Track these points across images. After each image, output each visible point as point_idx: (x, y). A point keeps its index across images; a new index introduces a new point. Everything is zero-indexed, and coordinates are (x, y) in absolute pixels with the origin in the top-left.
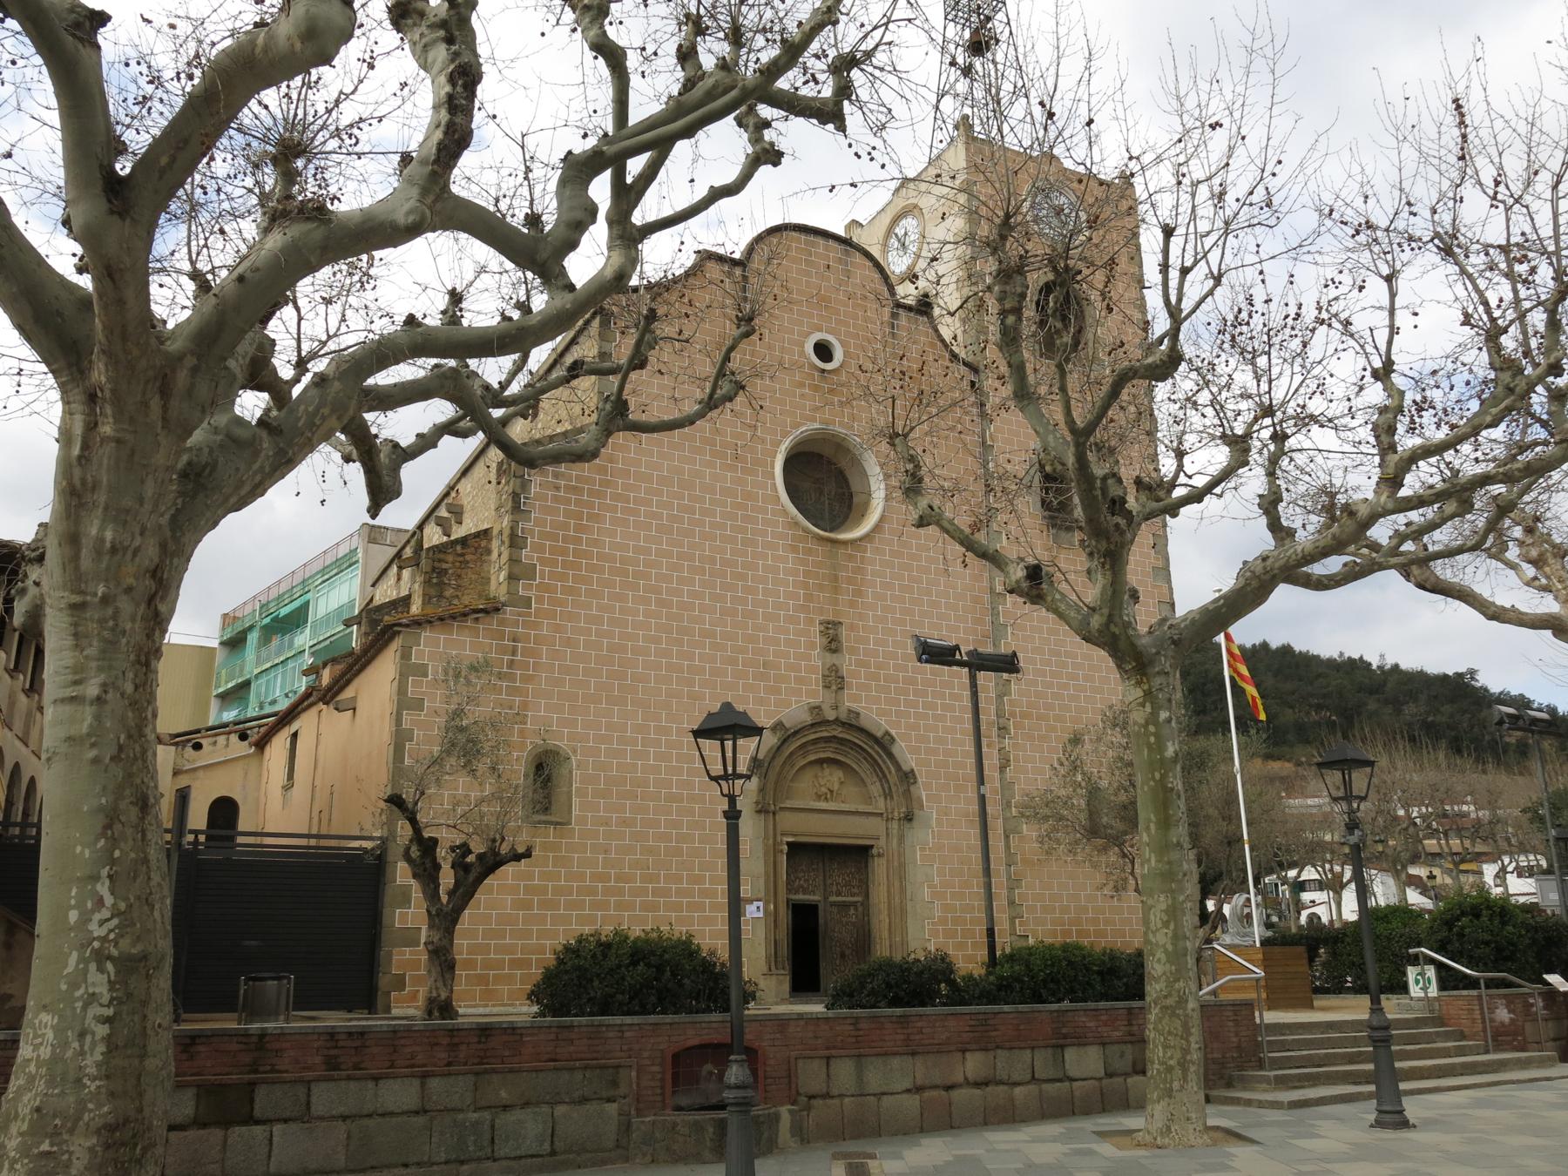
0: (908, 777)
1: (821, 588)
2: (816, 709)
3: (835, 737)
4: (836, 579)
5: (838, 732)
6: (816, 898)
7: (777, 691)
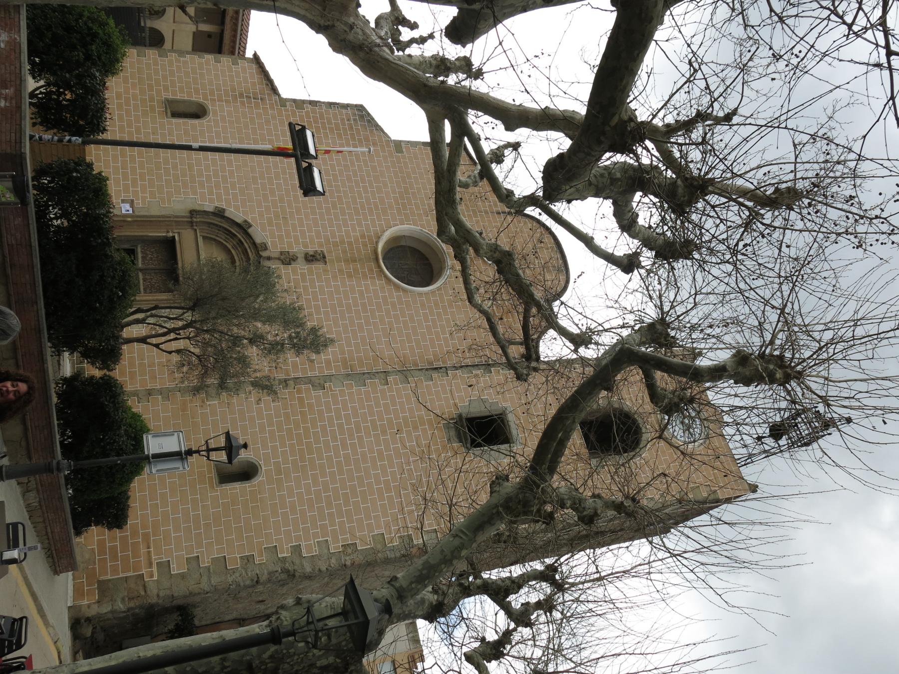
1: (344, 252)
2: (265, 247)
4: (355, 261)
6: (140, 265)
7: (270, 224)
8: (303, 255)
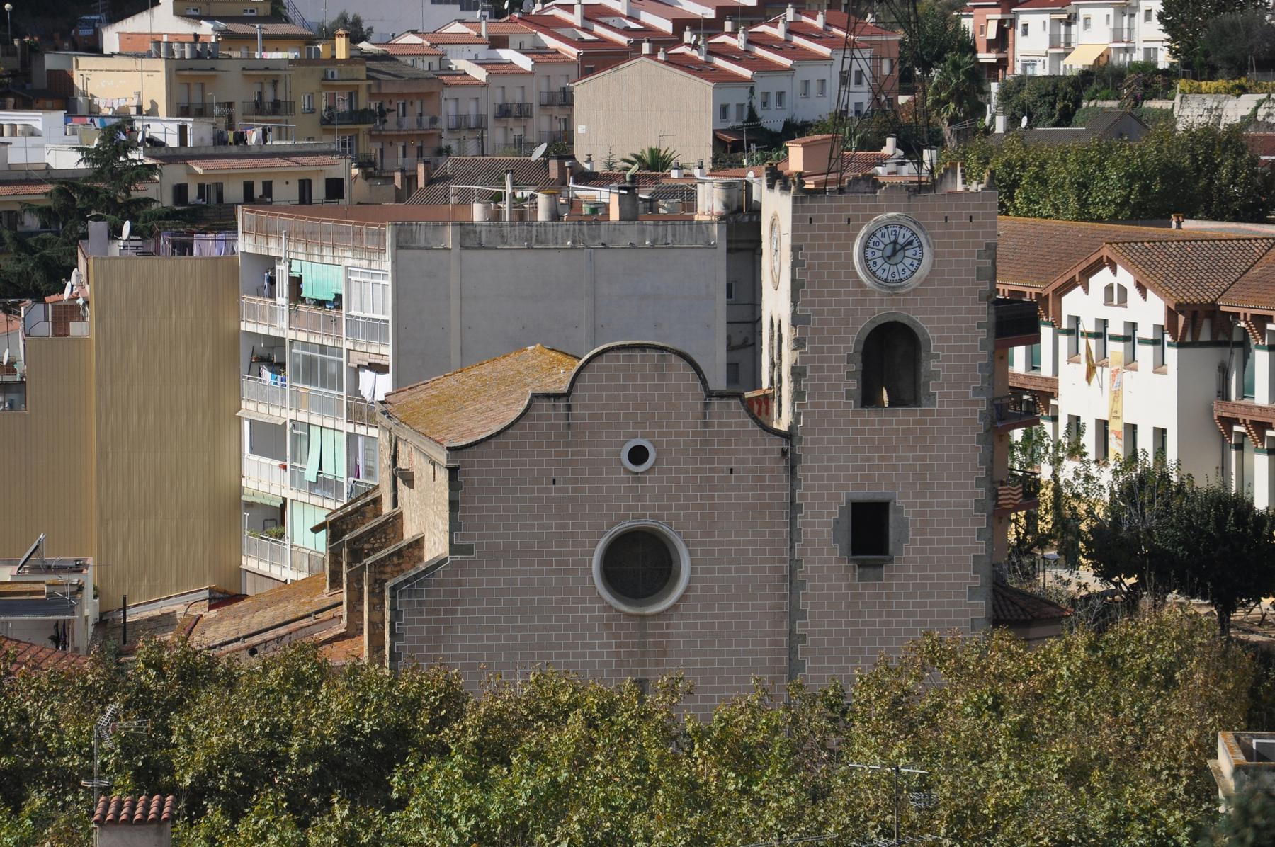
1: (631, 654)
4: (644, 643)
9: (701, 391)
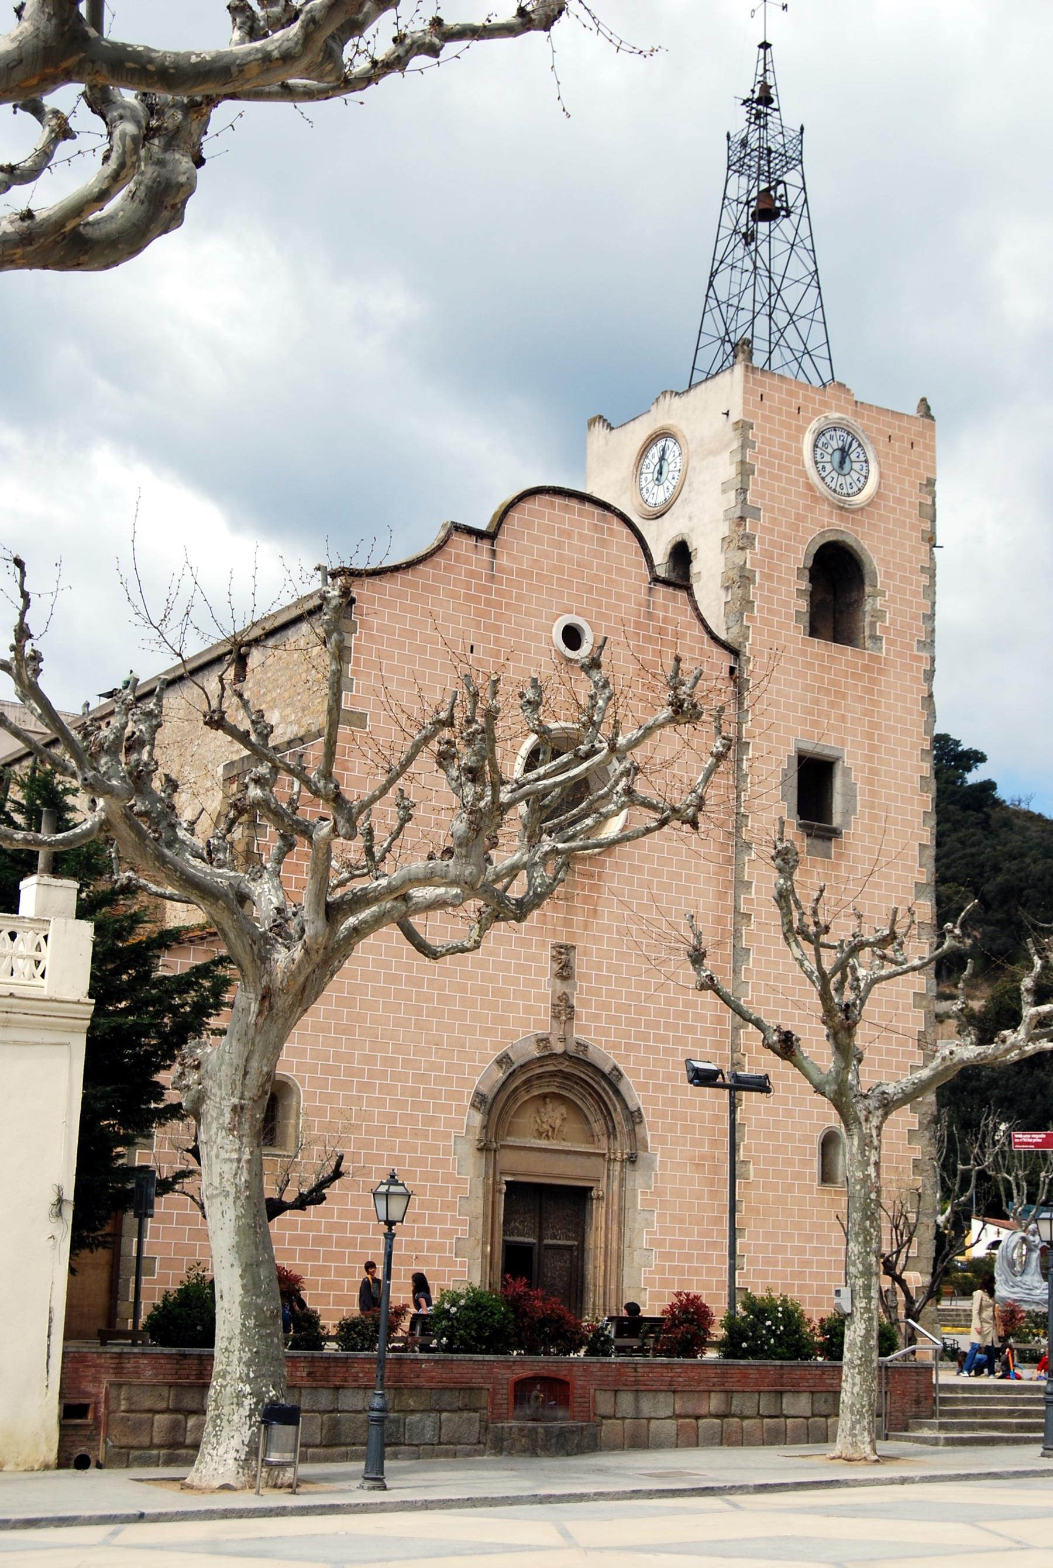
0: (634, 1117)
2: (543, 1041)
3: (561, 1071)
5: (566, 1067)
6: (531, 1240)
8: (558, 981)
9: (645, 571)
